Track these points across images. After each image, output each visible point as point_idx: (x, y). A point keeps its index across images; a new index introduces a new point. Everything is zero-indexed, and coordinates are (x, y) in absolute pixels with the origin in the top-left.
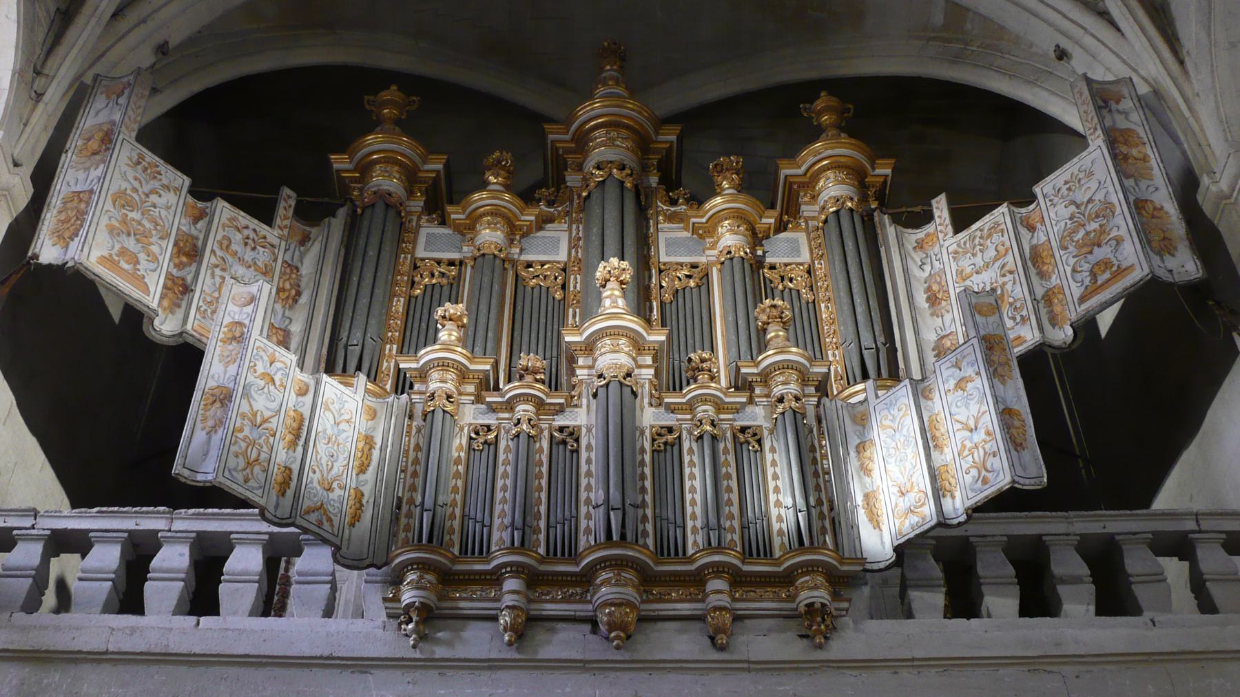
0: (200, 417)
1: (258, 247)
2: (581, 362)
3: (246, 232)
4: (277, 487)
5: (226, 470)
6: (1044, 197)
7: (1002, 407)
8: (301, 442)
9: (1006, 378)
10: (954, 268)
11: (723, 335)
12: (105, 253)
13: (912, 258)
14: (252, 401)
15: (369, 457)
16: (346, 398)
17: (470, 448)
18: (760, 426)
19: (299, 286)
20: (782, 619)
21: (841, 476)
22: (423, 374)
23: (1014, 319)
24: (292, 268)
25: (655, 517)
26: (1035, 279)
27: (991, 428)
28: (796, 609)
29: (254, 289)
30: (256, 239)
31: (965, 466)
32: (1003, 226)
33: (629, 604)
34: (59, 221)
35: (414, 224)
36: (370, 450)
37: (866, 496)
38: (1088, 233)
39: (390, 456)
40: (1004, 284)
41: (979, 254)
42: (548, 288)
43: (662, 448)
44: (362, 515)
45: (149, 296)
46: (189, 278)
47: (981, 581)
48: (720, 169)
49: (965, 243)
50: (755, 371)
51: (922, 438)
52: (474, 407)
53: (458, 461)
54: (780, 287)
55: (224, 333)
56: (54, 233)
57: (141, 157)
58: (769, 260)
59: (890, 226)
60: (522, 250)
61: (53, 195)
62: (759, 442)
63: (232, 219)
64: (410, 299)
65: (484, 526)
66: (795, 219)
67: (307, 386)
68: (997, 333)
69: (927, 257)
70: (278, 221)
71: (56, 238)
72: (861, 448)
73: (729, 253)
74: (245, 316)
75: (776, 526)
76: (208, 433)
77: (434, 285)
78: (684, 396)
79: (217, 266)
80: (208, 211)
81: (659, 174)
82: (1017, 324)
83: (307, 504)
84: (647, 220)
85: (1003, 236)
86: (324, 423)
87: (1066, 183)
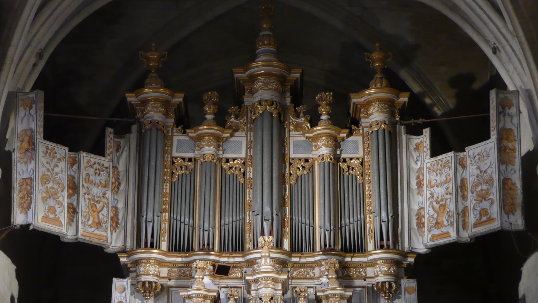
1: (101, 172)
2: (253, 288)
3: (95, 166)
10: (428, 178)
11: (318, 206)
12: (43, 215)
19: (119, 179)
23: (447, 221)
24: (115, 168)
26: (460, 199)
30: (99, 167)
32: (450, 164)
34: (20, 197)
38: (482, 190)
40: (446, 199)
45: (62, 227)
46: (75, 203)
48: (321, 99)
54: (347, 174)
56: (19, 205)
57: (47, 148)
58: (343, 156)
59: (404, 134)
61: (14, 182)
63: (89, 161)
66: (358, 127)
70: (108, 151)
71: (21, 209)
73: (323, 158)
74: (123, 298)
79: (85, 194)
80: (77, 159)
81: (291, 97)
82: (449, 225)
84: (285, 129)
85: (450, 170)
87: (478, 154)
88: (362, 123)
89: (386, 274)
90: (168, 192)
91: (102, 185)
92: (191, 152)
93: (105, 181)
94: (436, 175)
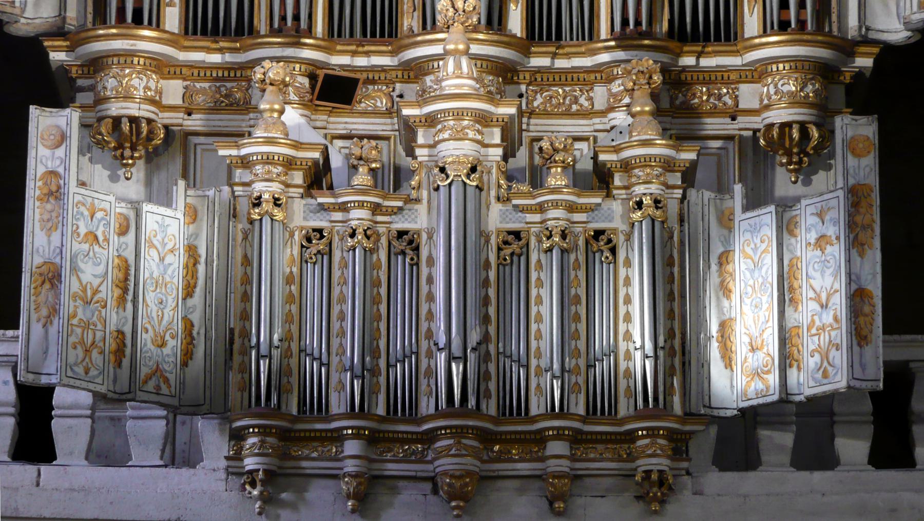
0: (33, 307)
2: (420, 140)
4: (112, 358)
5: (68, 367)
7: (854, 287)
8: (130, 297)
9: (866, 246)
14: (79, 273)
15: (194, 275)
17: (303, 261)
18: (615, 231)
22: (246, 163)
27: (839, 314)
33: (469, 473)
36: (194, 265)
37: (723, 325)
43: (509, 261)
44: (194, 350)
47: (836, 418)
51: (779, 290)
52: (303, 202)
55: (40, 188)
62: (613, 251)
65: (321, 364)
67: (127, 219)
68: (867, 182)
74: (58, 162)
76: (44, 326)
83: (144, 371)
86: (150, 266)
89: (795, 101)
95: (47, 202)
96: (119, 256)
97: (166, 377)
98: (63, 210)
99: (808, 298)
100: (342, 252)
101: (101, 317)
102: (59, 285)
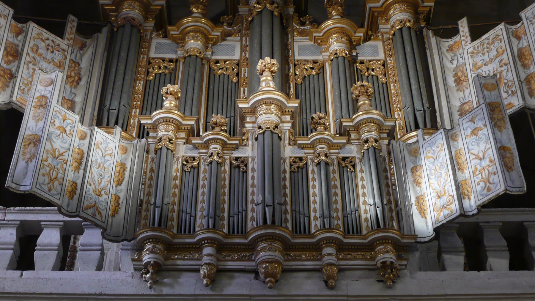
0: (21, 153)
1: (55, 51)
2: (248, 119)
3: (47, 42)
4: (68, 194)
5: (38, 184)
6: (527, 19)
7: (499, 145)
9: (502, 128)
11: (332, 103)
13: (446, 57)
14: (52, 142)
15: (123, 176)
16: (109, 141)
19: (80, 74)
20: (368, 271)
21: (402, 186)
22: (155, 127)
23: (507, 92)
24: (75, 63)
25: (292, 211)
26: (520, 69)
27: (492, 158)
28: (376, 265)
29: (53, 76)
30: (54, 46)
31: (477, 181)
32: (501, 37)
33: (277, 262)
35: (148, 37)
36: (123, 171)
37: (418, 199)
39: (136, 175)
40: (502, 72)
41: (487, 54)
42: (228, 76)
44: (119, 210)
46: (14, 70)
47: (486, 249)
49: (478, 47)
50: (351, 124)
51: (451, 164)
52: (185, 146)
53: (176, 178)
54: (367, 74)
55: (35, 102)
58: (360, 58)
60: (213, 53)
62: (354, 166)
63: (38, 34)
64: (147, 82)
65: (191, 216)
66: (375, 33)
67: (86, 134)
68: (496, 101)
69: (455, 55)
70: (67, 35)
72: (414, 170)
73: (336, 54)
74: (48, 92)
75: (363, 216)
76: (27, 162)
77: (160, 74)
78: (309, 139)
79: (30, 62)
80: (24, 29)
81: (294, 7)
82: (509, 95)
83: (86, 204)
84: (287, 35)
85: (501, 43)
86: (96, 155)
88: (380, 29)
90: (141, 89)
91: (54, 63)
92: (172, 54)
93: (60, 62)
94: (482, 56)
95: (38, 109)
96: (79, 149)
97: (100, 212)
98: (47, 112)
99: (471, 159)
100: (205, 166)
101: (62, 167)
102: (39, 145)
